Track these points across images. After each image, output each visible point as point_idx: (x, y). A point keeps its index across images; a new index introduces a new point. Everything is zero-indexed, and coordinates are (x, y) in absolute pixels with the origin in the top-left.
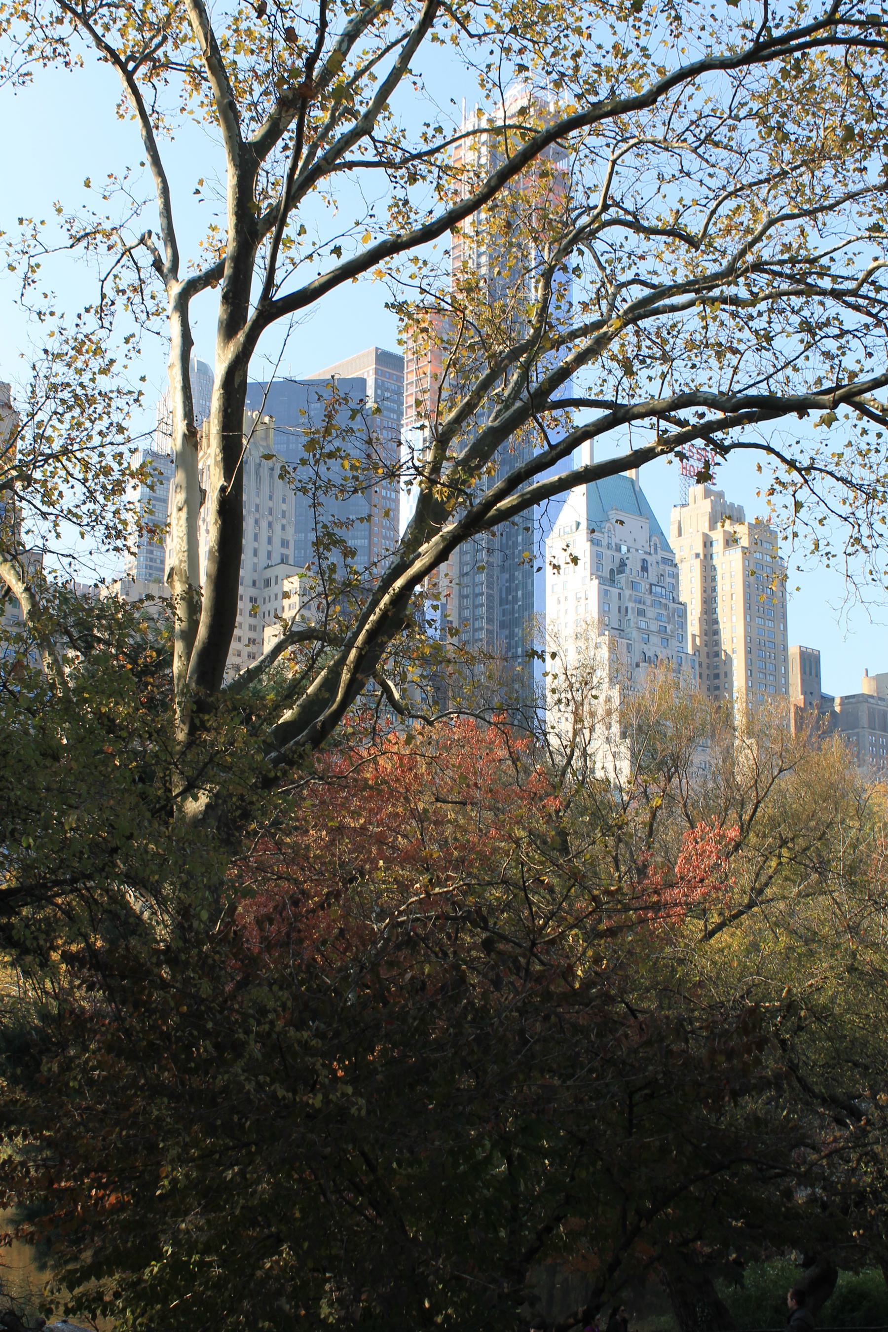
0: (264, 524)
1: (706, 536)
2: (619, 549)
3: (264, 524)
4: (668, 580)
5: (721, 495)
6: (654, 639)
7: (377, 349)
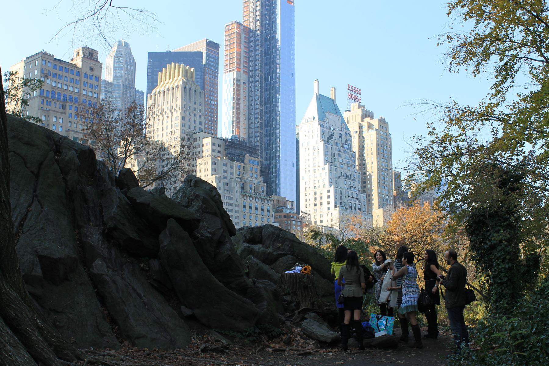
0: (193, 115)
1: (360, 124)
2: (330, 129)
3: (193, 115)
4: (348, 142)
5: (364, 107)
6: (345, 167)
7: (207, 40)
